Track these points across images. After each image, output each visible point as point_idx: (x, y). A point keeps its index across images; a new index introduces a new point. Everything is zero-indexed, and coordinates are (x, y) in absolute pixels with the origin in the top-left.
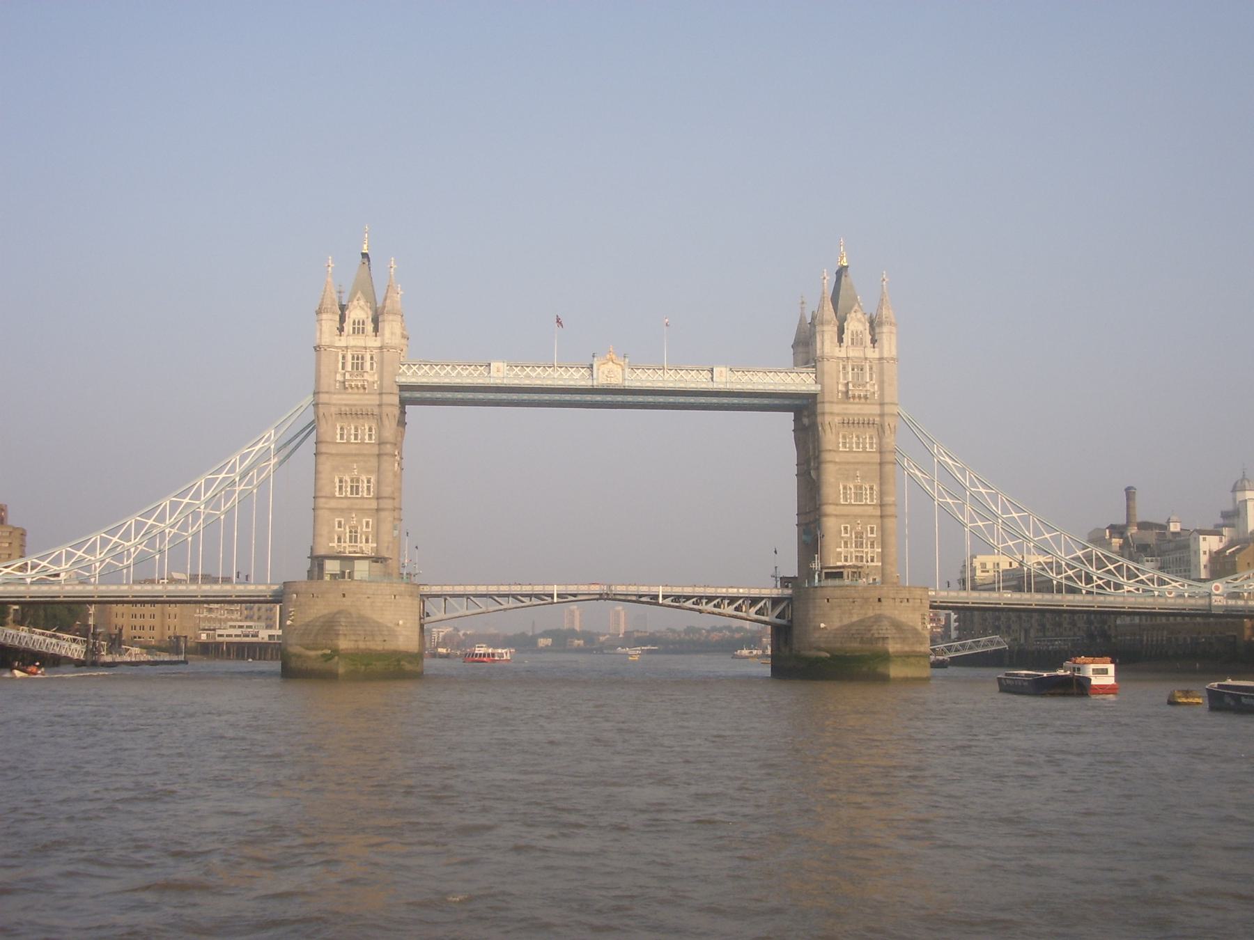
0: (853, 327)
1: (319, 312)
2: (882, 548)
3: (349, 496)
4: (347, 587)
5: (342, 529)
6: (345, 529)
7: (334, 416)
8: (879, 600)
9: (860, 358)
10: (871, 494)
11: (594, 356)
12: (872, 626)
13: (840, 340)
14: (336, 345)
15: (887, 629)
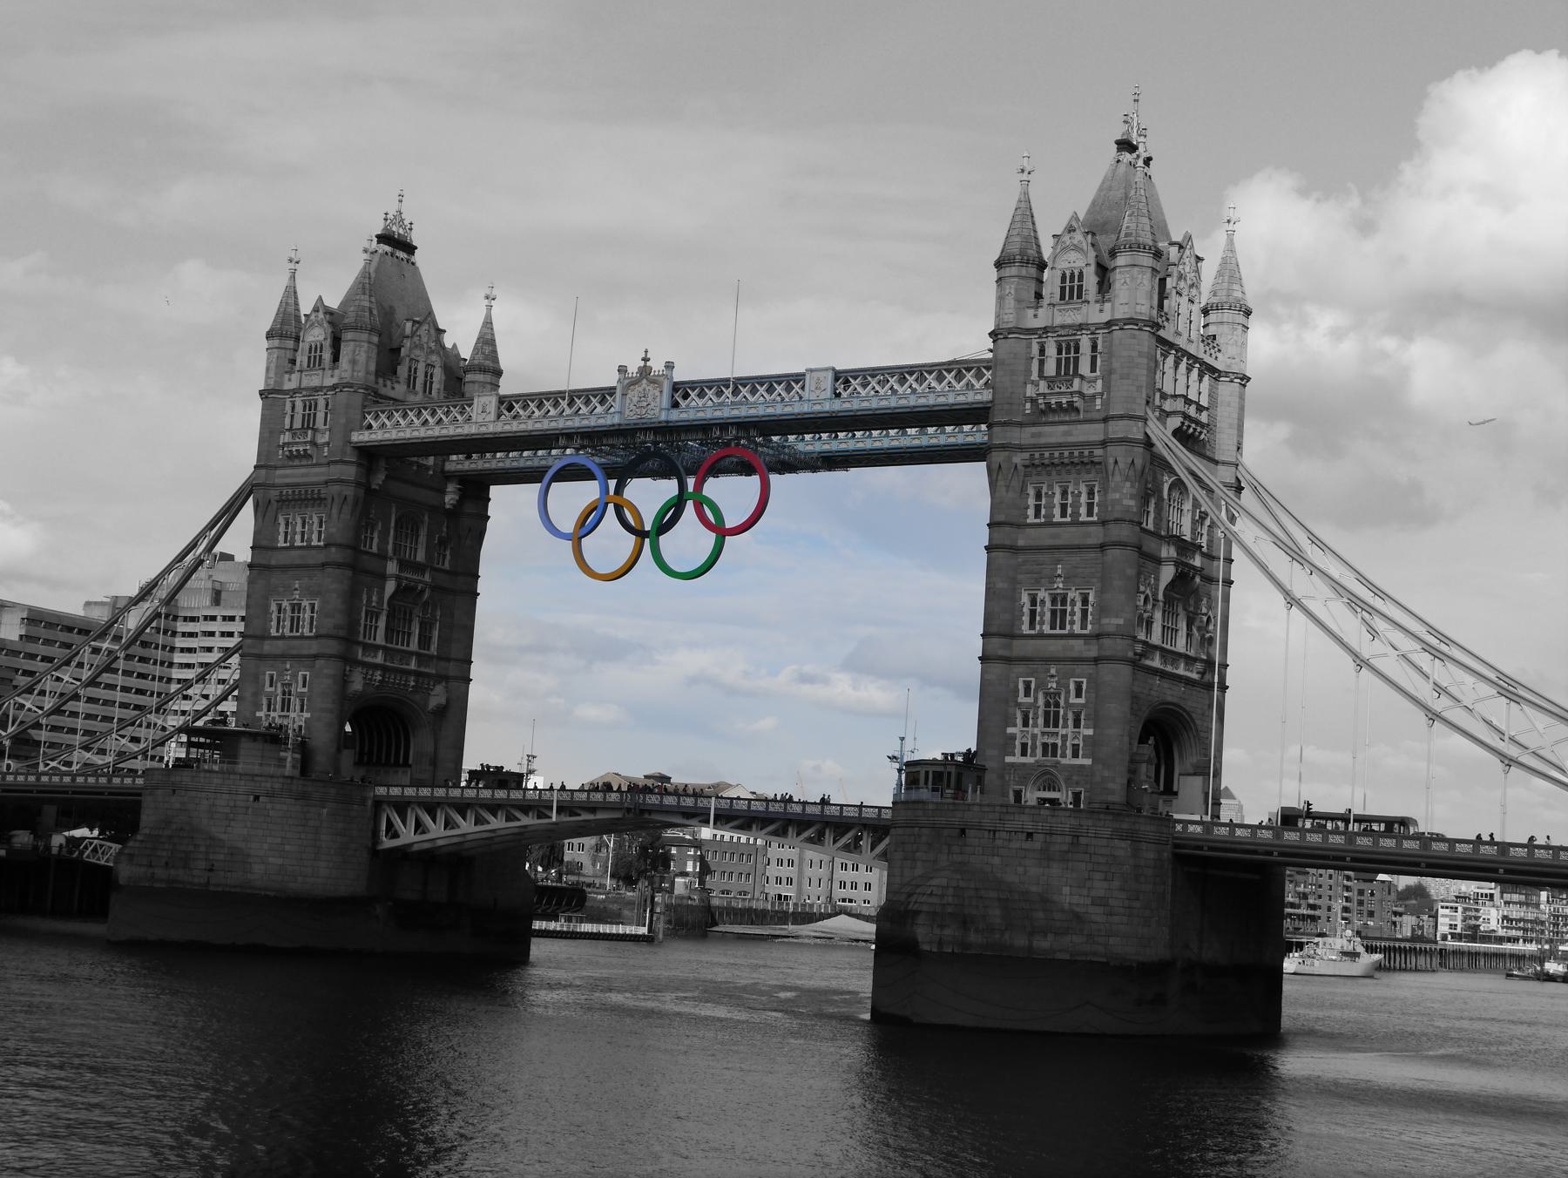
0: (1064, 265)
1: (269, 336)
2: (1094, 728)
3: (287, 632)
4: (178, 779)
5: (273, 689)
6: (276, 687)
7: (275, 505)
8: (963, 831)
9: (1069, 326)
10: (1084, 613)
11: (622, 370)
12: (918, 886)
13: (1039, 296)
14: (286, 387)
15: (931, 894)
